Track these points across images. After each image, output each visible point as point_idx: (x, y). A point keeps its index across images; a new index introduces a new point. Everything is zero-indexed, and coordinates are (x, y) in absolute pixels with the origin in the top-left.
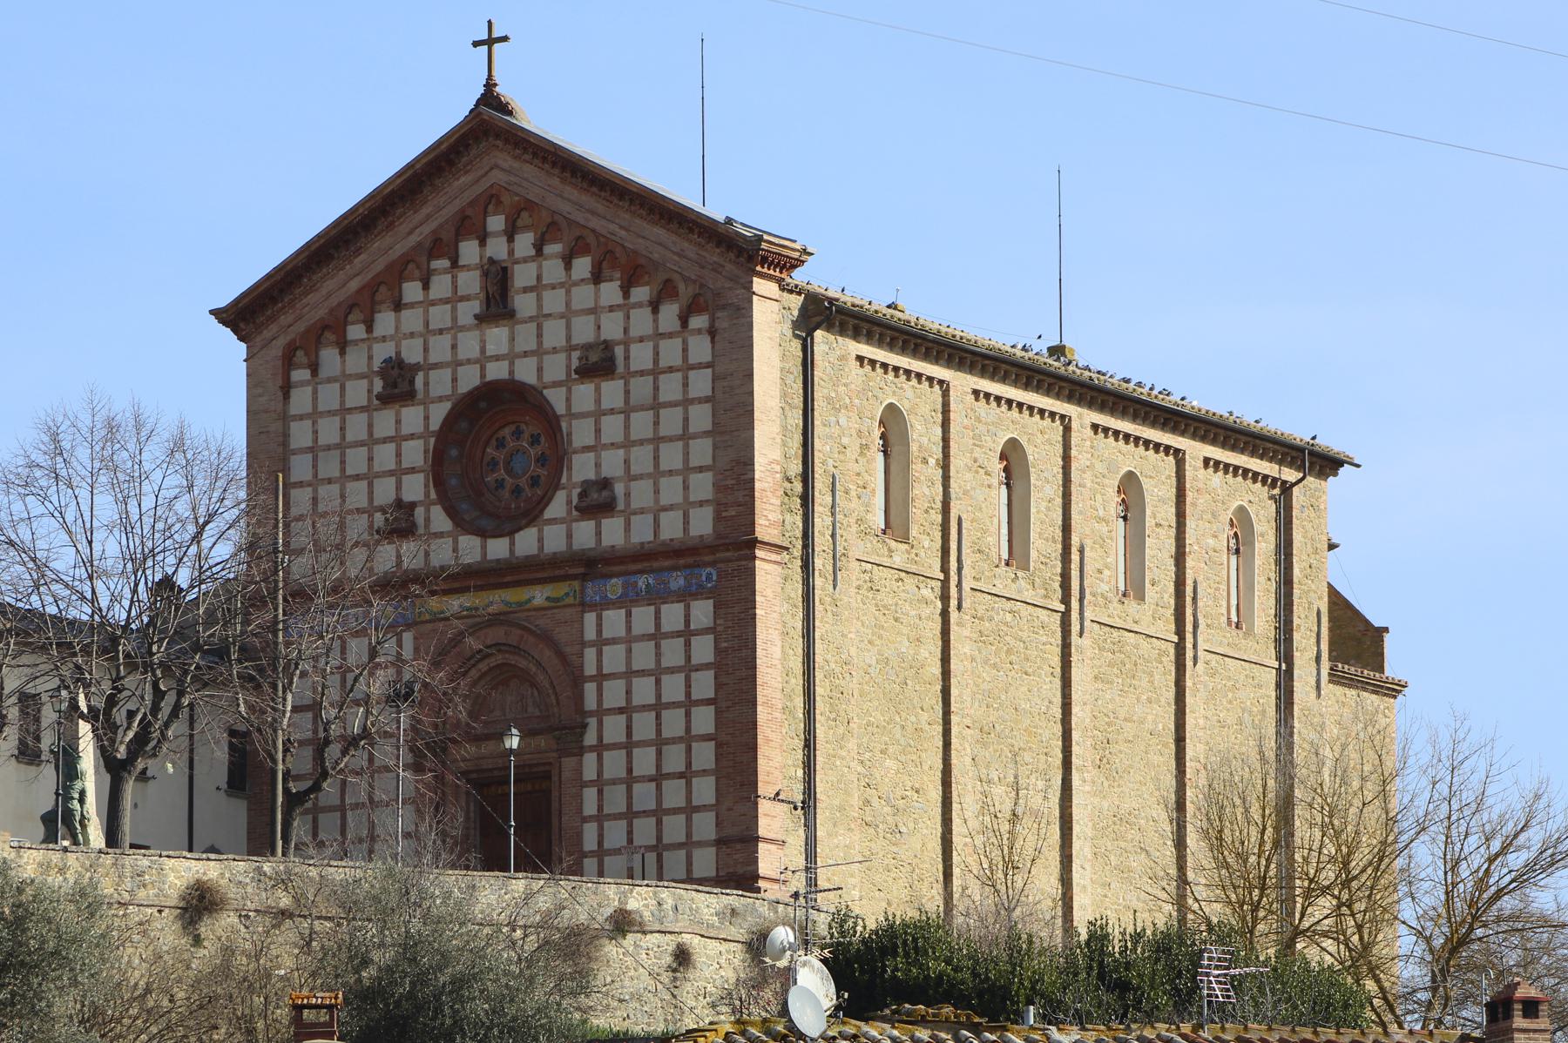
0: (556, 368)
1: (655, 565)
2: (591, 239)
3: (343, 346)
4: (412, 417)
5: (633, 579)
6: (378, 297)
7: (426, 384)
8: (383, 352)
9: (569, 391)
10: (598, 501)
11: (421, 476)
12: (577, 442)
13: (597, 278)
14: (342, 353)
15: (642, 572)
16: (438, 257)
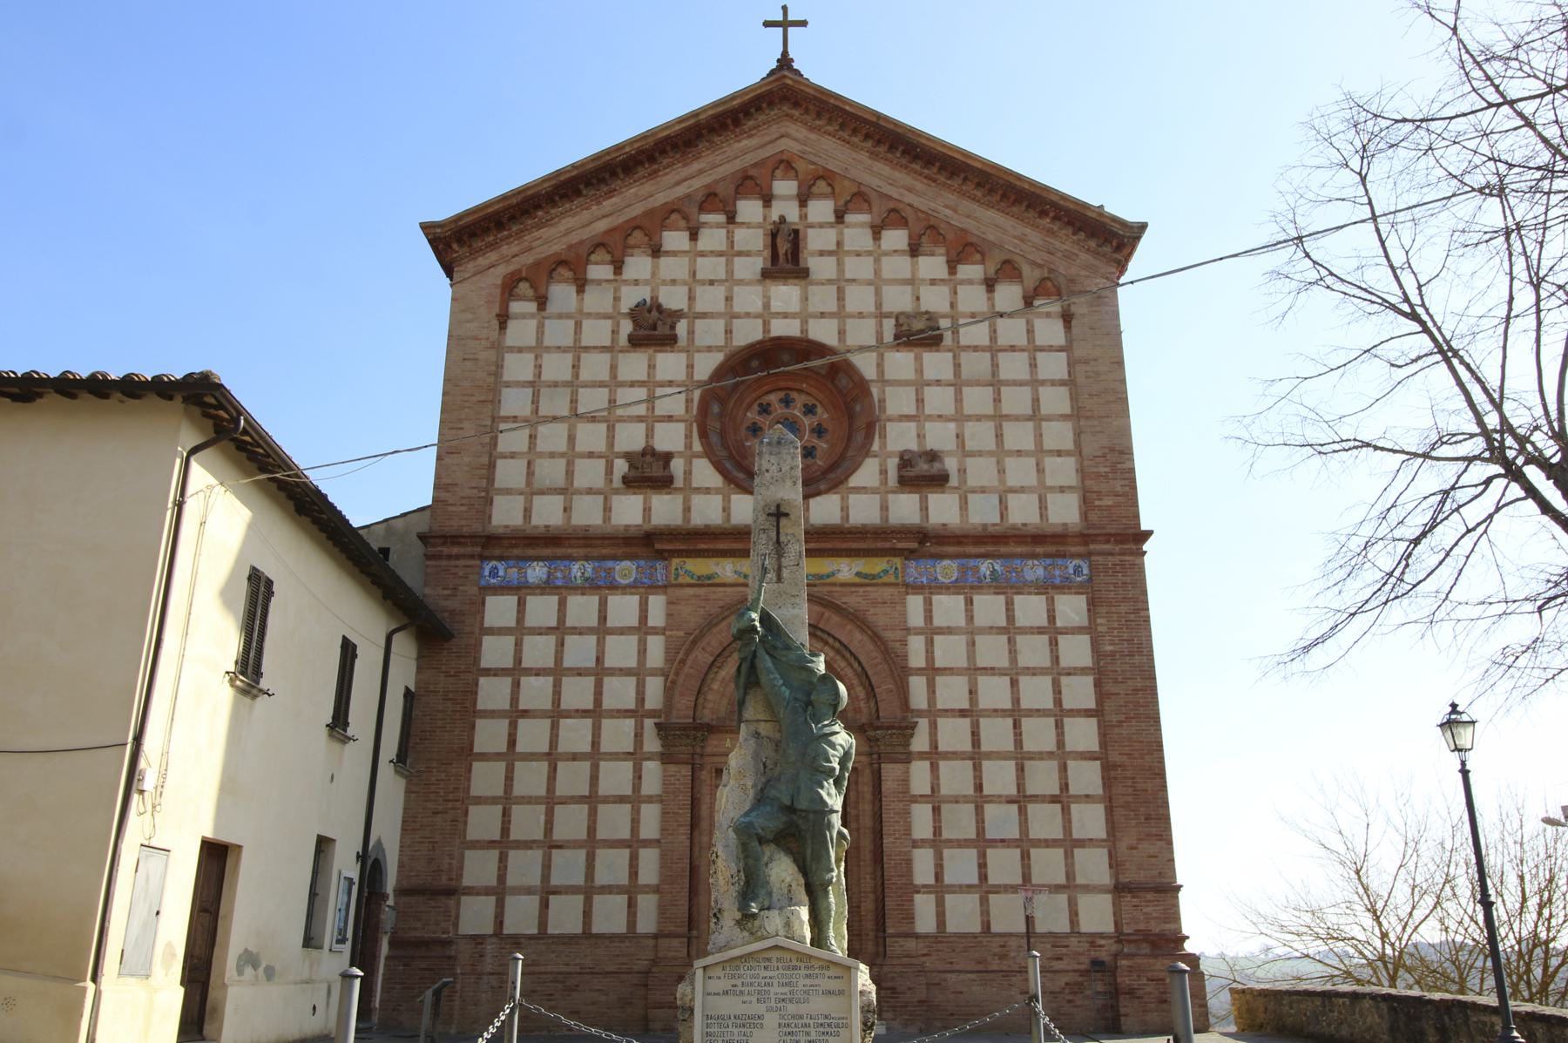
0: (862, 333)
1: (1003, 549)
2: (908, 213)
3: (581, 284)
4: (670, 364)
5: (972, 563)
6: (631, 241)
7: (691, 332)
8: (631, 297)
9: (881, 357)
10: (921, 474)
11: (681, 426)
12: (891, 409)
13: (914, 251)
14: (581, 290)
15: (985, 556)
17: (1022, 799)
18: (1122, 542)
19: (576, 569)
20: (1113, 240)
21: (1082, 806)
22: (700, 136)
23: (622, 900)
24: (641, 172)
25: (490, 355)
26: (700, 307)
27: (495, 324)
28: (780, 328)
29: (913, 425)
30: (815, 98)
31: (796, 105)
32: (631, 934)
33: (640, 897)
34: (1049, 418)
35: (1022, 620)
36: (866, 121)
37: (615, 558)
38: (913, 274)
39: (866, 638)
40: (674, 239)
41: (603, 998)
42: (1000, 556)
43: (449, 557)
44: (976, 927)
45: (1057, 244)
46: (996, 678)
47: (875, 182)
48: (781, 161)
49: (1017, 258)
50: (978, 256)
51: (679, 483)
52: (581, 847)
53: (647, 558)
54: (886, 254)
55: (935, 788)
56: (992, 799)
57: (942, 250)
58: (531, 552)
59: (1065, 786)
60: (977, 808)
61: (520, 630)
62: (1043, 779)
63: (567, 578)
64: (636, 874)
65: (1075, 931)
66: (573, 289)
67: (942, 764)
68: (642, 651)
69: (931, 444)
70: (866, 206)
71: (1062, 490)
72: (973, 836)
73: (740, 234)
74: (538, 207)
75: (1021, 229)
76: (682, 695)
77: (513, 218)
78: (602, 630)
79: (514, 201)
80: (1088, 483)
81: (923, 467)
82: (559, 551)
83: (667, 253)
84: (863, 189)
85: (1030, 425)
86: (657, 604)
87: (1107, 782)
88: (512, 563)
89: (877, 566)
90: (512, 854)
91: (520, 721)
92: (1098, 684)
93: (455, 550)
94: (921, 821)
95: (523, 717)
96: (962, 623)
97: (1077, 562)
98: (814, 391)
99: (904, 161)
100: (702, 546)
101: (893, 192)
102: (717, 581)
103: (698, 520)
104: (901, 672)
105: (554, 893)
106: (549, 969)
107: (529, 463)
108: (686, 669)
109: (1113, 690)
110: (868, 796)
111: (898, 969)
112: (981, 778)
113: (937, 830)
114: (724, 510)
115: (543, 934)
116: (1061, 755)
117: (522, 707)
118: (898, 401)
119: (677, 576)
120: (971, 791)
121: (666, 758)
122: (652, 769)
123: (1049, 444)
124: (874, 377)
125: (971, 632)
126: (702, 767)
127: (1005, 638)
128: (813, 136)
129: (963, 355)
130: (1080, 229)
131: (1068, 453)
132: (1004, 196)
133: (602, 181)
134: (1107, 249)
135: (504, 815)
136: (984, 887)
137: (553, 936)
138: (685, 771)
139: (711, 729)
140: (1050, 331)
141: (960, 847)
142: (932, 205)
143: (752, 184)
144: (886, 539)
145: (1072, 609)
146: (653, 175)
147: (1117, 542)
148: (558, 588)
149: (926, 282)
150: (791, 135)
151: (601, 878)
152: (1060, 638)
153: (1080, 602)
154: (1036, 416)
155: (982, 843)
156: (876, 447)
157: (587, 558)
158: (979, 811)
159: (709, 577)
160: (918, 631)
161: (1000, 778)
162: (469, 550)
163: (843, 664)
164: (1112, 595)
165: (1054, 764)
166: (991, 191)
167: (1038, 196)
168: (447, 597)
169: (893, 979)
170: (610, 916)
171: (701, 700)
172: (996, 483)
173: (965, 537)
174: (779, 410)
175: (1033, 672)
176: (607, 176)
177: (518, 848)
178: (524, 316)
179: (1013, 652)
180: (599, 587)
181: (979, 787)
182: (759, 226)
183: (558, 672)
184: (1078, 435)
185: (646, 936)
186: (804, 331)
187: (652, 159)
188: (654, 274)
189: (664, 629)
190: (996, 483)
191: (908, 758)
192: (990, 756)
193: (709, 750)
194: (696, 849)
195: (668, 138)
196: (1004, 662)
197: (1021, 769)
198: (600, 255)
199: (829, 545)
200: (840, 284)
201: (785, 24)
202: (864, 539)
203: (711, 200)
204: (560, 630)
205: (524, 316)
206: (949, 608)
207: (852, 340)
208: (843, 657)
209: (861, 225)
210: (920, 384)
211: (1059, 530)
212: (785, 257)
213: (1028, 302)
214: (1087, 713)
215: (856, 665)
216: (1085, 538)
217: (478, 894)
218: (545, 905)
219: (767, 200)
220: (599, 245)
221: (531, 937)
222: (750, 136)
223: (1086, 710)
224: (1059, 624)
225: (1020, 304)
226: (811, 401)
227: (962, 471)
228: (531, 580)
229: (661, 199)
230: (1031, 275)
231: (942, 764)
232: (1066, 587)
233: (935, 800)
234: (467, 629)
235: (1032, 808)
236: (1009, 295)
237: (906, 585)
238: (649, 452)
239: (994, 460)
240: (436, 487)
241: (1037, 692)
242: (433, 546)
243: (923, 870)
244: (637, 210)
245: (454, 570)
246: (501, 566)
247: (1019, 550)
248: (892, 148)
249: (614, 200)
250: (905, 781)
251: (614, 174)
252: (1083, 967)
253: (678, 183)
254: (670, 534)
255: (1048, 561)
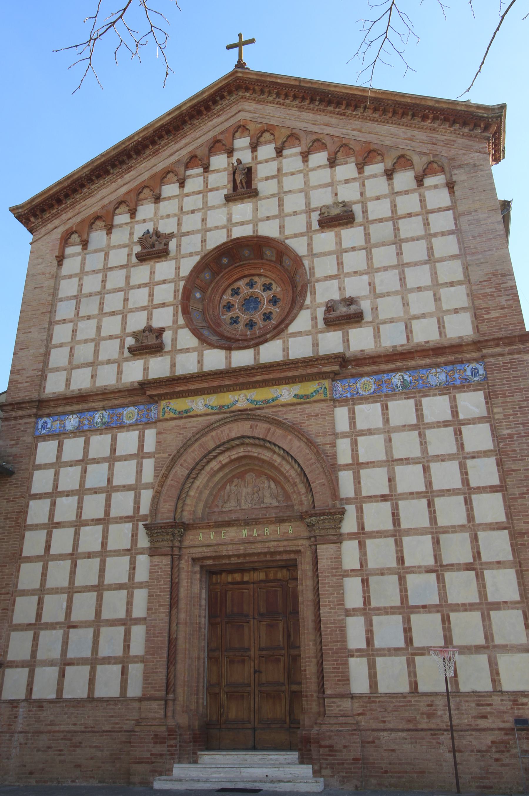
0: (296, 225)
1: (411, 363)
2: (328, 141)
3: (109, 229)
4: (164, 269)
5: (386, 377)
6: (142, 196)
7: (179, 246)
8: (139, 231)
9: (311, 239)
10: (344, 316)
11: (170, 309)
12: (319, 273)
13: (332, 163)
14: (109, 233)
15: (396, 370)
16: (192, 168)
17: (439, 569)
18: (511, 344)
19: (97, 417)
20: (484, 125)
21: (495, 572)
22: (184, 122)
23: (117, 669)
24: (148, 152)
25: (52, 282)
26: (185, 229)
27: (55, 262)
28: (238, 232)
29: (335, 282)
30: (258, 80)
31: (247, 89)
32: (123, 698)
33: (131, 666)
34: (442, 260)
35: (429, 417)
36: (292, 86)
37: (123, 406)
38: (332, 179)
39: (303, 445)
40: (170, 189)
41: (99, 754)
42: (408, 369)
43: (16, 418)
44: (405, 688)
45: (439, 137)
46: (410, 467)
47: (303, 125)
48: (239, 127)
49: (408, 153)
50: (379, 158)
51: (168, 347)
52: (90, 626)
53: (145, 403)
54: (313, 170)
55: (363, 563)
56: (412, 570)
57: (353, 159)
58: (69, 408)
59: (477, 555)
60: (400, 578)
61: (58, 464)
62: (457, 549)
63: (91, 424)
64: (129, 646)
65: (497, 691)
66: (104, 233)
67: (368, 542)
68: (139, 472)
69: (349, 293)
70: (297, 142)
71: (456, 311)
72: (398, 604)
73: (212, 178)
74: (83, 186)
75: (410, 132)
76: (165, 501)
77: (67, 196)
78: (113, 458)
79: (66, 184)
80: (477, 302)
81: (343, 310)
82: (86, 406)
83: (165, 199)
84: (294, 131)
85: (427, 267)
86: (150, 435)
87: (515, 548)
88: (56, 418)
89: (309, 388)
90: (42, 633)
91: (54, 531)
92: (500, 464)
93: (20, 413)
94: (353, 593)
95: (56, 527)
96: (380, 424)
97: (473, 365)
98: (268, 273)
99: (321, 107)
100: (180, 389)
101: (316, 129)
102: (191, 413)
103: (180, 371)
104: (332, 468)
105: (69, 664)
106: (62, 728)
107: (71, 348)
108: (169, 482)
109: (513, 467)
110: (310, 574)
111: (335, 728)
112: (402, 551)
113: (367, 600)
114: (199, 362)
115: (59, 699)
116: (472, 527)
117: (56, 520)
118: (324, 267)
119: (164, 413)
120: (394, 564)
121: (153, 552)
122: (143, 560)
123: (443, 278)
124: (306, 253)
125: (388, 431)
126: (180, 557)
127: (416, 433)
128: (260, 107)
129: (371, 226)
130: (454, 122)
131: (459, 283)
132: (395, 113)
133: (122, 162)
134: (478, 131)
135: (39, 603)
136: (410, 650)
137: (67, 701)
138: (166, 561)
139: (187, 527)
140: (438, 197)
141: (387, 614)
142: (344, 131)
143: (220, 145)
144: (313, 366)
145: (472, 403)
146: (156, 153)
147: (506, 345)
148: (84, 431)
149: (344, 183)
150: (248, 110)
151: (104, 652)
152: (463, 428)
153: (479, 396)
154: (431, 260)
155: (406, 609)
156: (308, 302)
157: (104, 408)
158: (402, 581)
159: (186, 412)
160: (345, 435)
161: (419, 551)
162: (29, 412)
163: (288, 467)
164: (505, 388)
165: (467, 535)
166: (385, 112)
167: (418, 105)
168: (12, 446)
169: (330, 737)
170: (108, 684)
171: (180, 505)
172: (402, 314)
173: (379, 357)
174: (245, 291)
175: (442, 458)
176: (125, 158)
177: (46, 629)
178: (74, 255)
179: (424, 444)
180: (112, 428)
181: (401, 560)
182: (225, 170)
183: (81, 492)
184: (466, 268)
185: (133, 699)
186: (255, 231)
187: (154, 143)
188: (155, 214)
189: (154, 453)
190: (402, 314)
191: (339, 539)
192: (409, 532)
193: (186, 543)
194: (174, 624)
195: (162, 126)
196: (417, 453)
197: (436, 542)
198: (123, 208)
199: (271, 376)
200: (280, 197)
201: (239, 45)
202: (296, 368)
203: (192, 160)
204: (85, 462)
205: (74, 255)
206: (369, 414)
207: (288, 232)
208: (288, 462)
209: (294, 155)
210: (340, 252)
211: (457, 341)
212: (243, 186)
213: (420, 181)
214: (493, 489)
215: (296, 466)
216: (477, 345)
217: (17, 667)
218: (62, 674)
219: (230, 152)
220: (121, 202)
221: (51, 702)
222: (219, 116)
223: (491, 487)
224: (461, 416)
225: (413, 184)
226: (268, 281)
227: (375, 309)
228: (67, 428)
229: (161, 166)
230: (420, 162)
231: (368, 542)
232: (466, 386)
233: (364, 574)
234: (23, 467)
235: (448, 576)
236: (404, 179)
237: (333, 400)
238: (149, 329)
239: (399, 297)
240: (12, 372)
241: (446, 475)
242: (7, 412)
243: (356, 639)
244: (146, 176)
245: (18, 427)
246: (49, 420)
247: (424, 362)
248: (312, 100)
249: (131, 173)
250: (338, 558)
251: (130, 157)
252: (507, 725)
253: (171, 155)
254: (159, 383)
255: (449, 368)
